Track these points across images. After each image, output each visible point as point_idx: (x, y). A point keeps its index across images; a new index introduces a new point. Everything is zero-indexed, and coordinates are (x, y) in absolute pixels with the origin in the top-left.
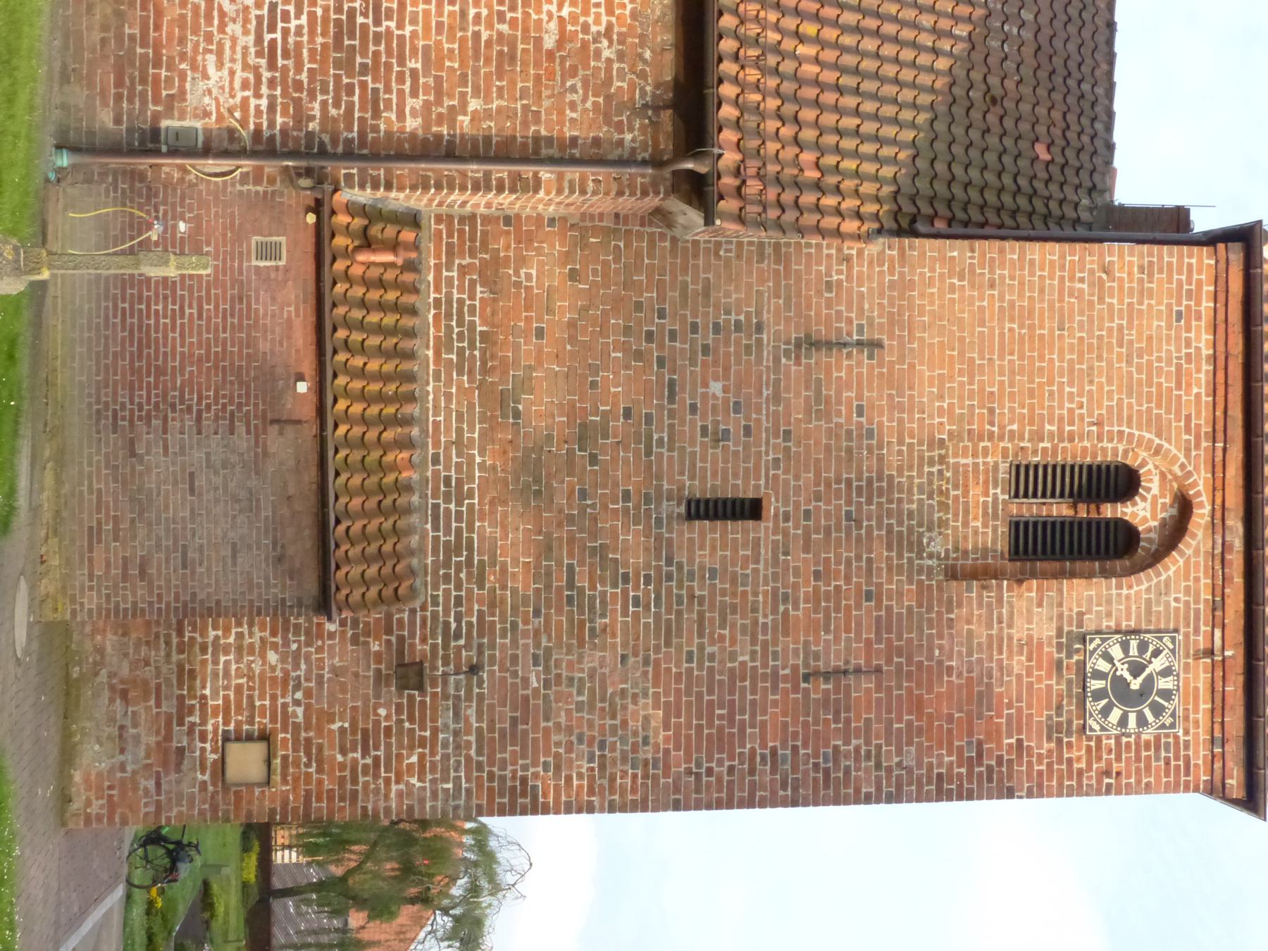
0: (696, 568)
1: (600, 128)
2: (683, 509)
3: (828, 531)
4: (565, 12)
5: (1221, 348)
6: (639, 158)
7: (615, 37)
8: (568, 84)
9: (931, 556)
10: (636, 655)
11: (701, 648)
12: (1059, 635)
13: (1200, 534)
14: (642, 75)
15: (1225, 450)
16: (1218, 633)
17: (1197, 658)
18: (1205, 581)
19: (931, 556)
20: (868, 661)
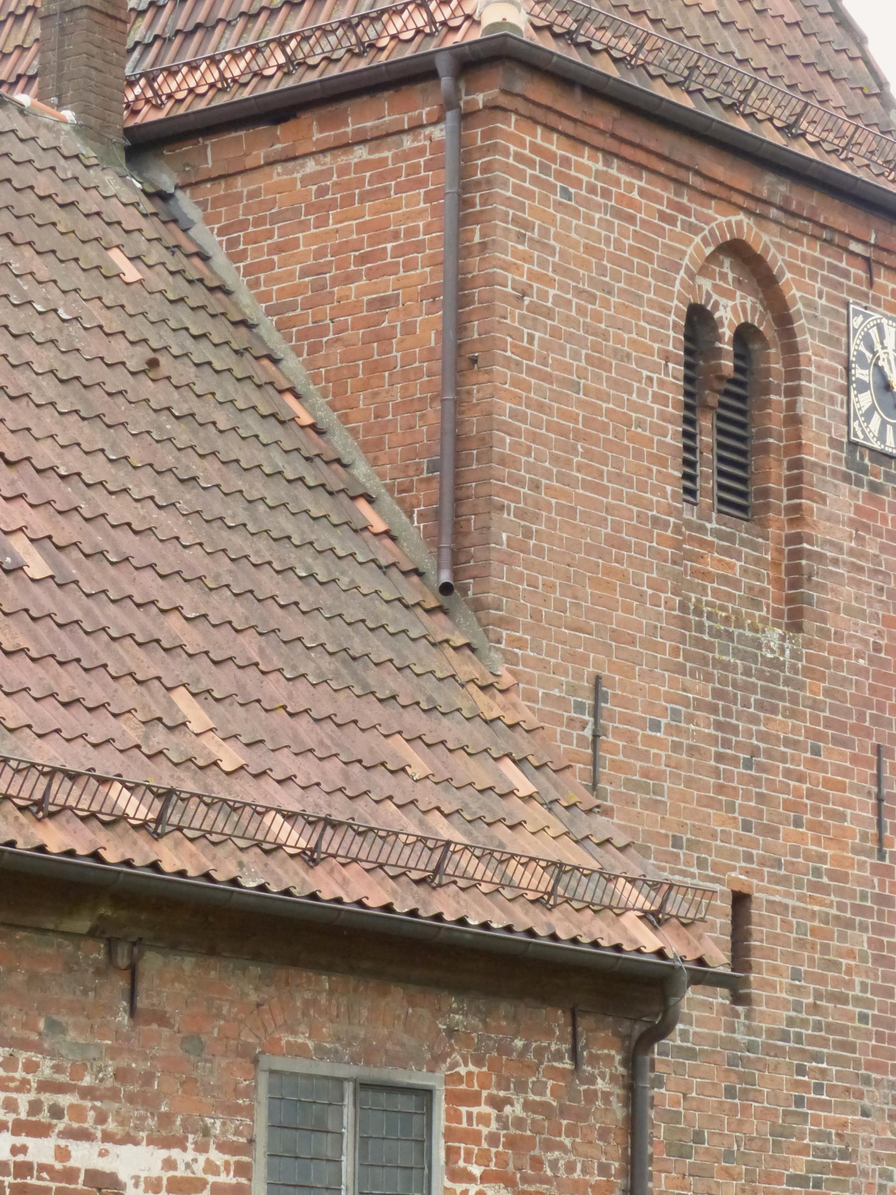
0: (791, 998)
1: (591, 1127)
2: (740, 1009)
3: (761, 798)
4: (476, 1170)
5: (598, 140)
6: (621, 1070)
7: (502, 1094)
8: (549, 1173)
9: (782, 650)
10: (860, 1095)
11: (858, 1001)
12: (846, 478)
13: (765, 238)
14: (540, 1052)
15: (698, 173)
16: (854, 247)
17: (871, 284)
18: (804, 248)
19: (782, 650)
20: (866, 763)
